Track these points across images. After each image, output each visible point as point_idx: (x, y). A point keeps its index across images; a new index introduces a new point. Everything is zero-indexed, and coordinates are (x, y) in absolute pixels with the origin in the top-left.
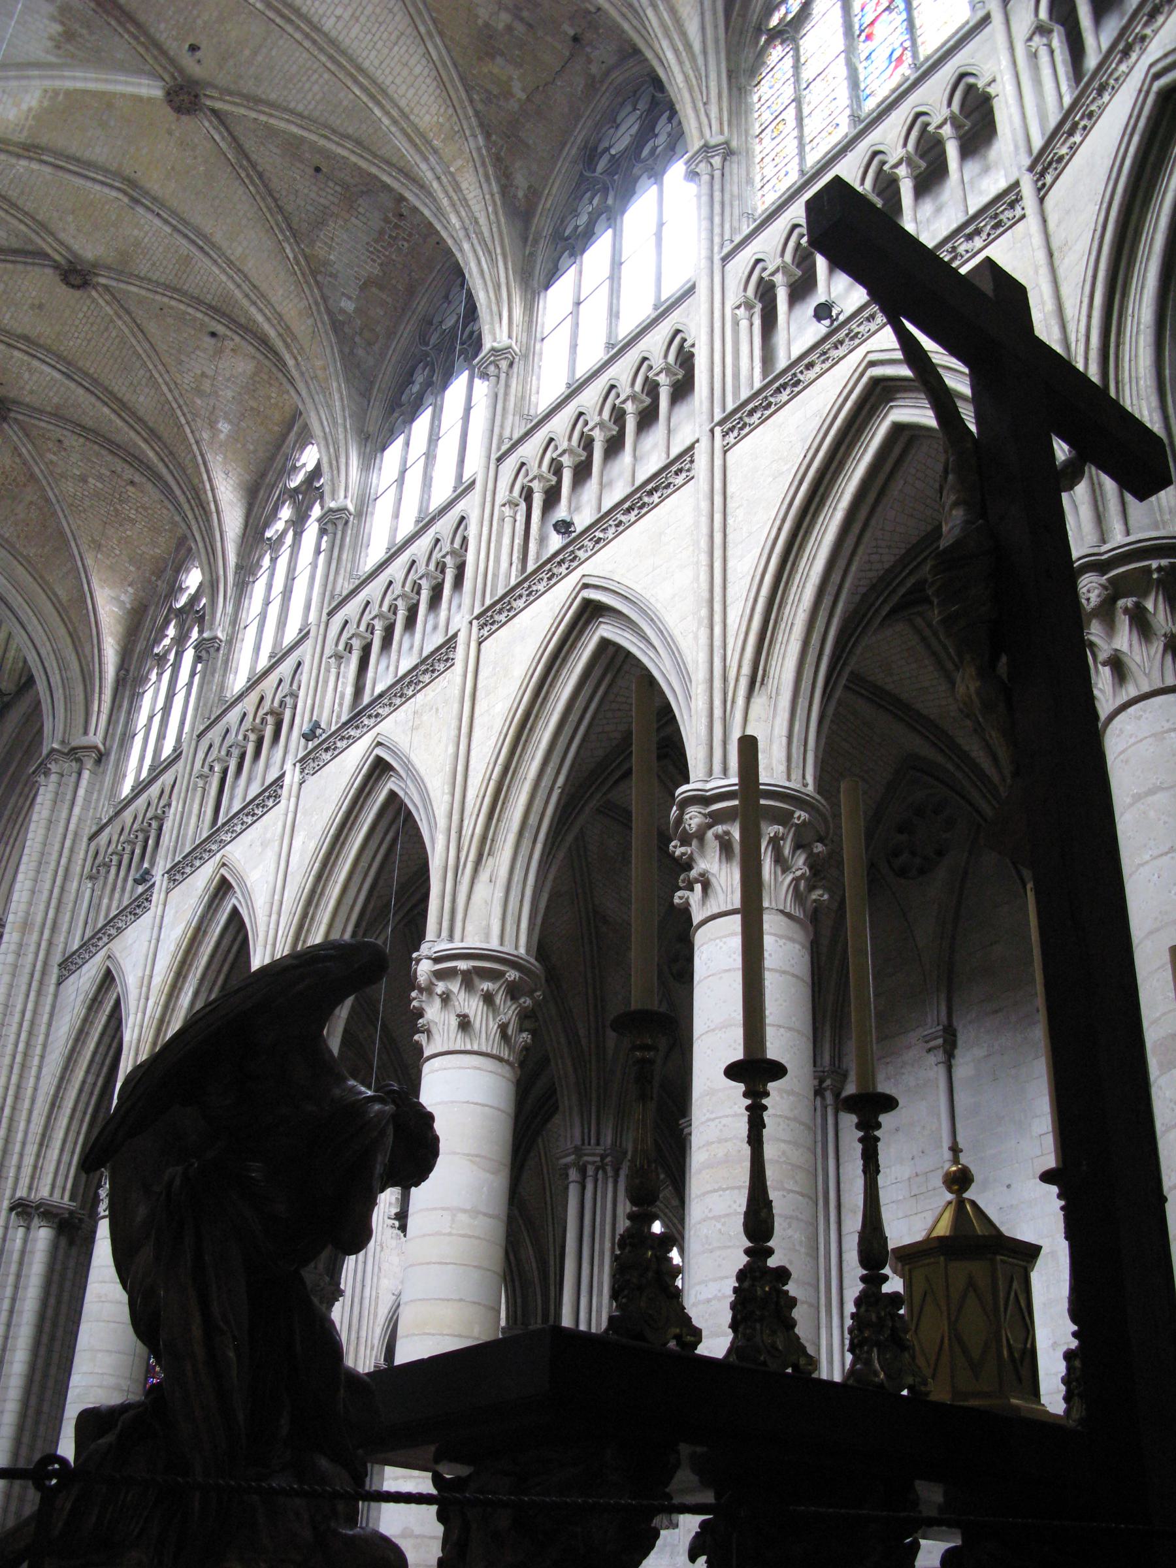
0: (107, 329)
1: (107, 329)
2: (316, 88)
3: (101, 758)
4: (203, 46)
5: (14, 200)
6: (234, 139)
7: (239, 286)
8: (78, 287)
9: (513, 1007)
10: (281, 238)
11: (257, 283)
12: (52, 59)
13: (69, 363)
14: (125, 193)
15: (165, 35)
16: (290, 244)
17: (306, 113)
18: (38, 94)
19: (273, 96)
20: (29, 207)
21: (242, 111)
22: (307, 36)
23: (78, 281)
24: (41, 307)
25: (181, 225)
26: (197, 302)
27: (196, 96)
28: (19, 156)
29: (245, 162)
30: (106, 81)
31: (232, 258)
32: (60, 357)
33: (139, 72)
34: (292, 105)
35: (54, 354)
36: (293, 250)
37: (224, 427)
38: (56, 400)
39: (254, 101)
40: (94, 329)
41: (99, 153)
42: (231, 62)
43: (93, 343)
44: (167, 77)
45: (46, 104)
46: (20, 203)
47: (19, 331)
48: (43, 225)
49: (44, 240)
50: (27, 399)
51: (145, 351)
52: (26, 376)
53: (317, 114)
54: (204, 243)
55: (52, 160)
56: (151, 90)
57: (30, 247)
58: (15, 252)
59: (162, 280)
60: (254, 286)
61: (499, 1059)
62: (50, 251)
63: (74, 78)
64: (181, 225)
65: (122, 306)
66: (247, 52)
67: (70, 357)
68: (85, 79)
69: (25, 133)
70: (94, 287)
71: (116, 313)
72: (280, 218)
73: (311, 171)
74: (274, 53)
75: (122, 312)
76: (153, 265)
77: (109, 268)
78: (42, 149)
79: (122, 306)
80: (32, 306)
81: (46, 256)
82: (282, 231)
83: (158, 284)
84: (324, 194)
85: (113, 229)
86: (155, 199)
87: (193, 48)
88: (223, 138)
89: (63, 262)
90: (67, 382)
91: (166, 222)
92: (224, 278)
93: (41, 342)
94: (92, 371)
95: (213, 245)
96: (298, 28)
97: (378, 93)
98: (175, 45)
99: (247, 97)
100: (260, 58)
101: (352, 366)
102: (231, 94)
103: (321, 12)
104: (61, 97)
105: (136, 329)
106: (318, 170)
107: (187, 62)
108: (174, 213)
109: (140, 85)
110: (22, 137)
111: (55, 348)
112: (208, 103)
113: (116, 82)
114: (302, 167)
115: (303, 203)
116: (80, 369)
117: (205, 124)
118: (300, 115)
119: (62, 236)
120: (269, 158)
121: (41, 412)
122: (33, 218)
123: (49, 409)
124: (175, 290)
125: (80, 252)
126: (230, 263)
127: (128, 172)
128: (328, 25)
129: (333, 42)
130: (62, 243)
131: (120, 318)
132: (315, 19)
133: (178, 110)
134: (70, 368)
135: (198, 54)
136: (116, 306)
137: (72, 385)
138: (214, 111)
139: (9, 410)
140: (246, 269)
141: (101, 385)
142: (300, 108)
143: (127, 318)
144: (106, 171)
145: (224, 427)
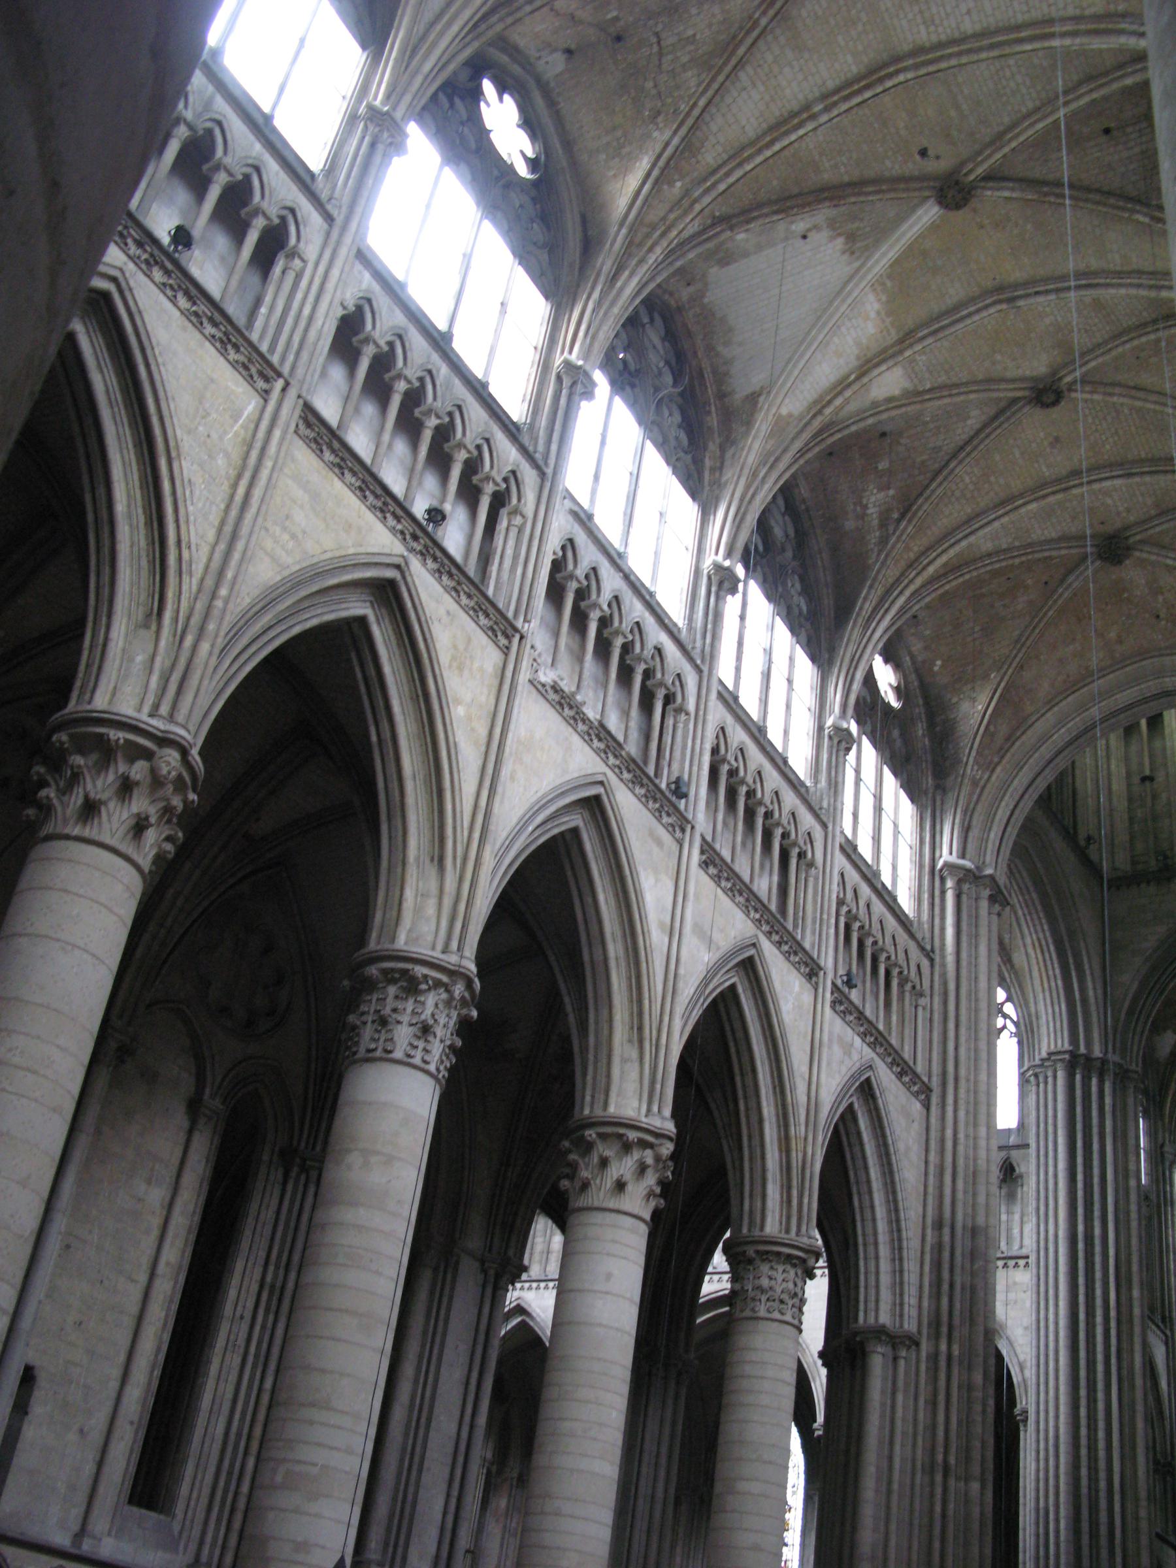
0: (1117, 412)
1: (1117, 412)
2: (1019, 78)
4: (925, 143)
5: (949, 382)
6: (1021, 180)
7: (1139, 286)
8: (1055, 403)
10: (1127, 215)
11: (1151, 269)
12: (857, 264)
13: (1121, 464)
14: (1000, 302)
15: (897, 167)
16: (1138, 212)
17: (1038, 103)
18: (871, 297)
19: (1006, 120)
20: (964, 376)
21: (998, 155)
22: (959, 54)
23: (1052, 397)
24: (1057, 440)
26: (1141, 327)
27: (957, 183)
28: (901, 352)
29: (1045, 189)
30: (898, 240)
31: (1118, 268)
32: (1111, 465)
33: (914, 209)
34: (1024, 110)
36: (1145, 215)
38: (1149, 501)
40: (1109, 419)
41: (955, 292)
42: (955, 133)
43: (1121, 432)
44: (927, 193)
45: (884, 298)
46: (955, 380)
47: (1064, 472)
48: (989, 380)
49: (998, 390)
50: (1132, 518)
51: (1156, 403)
52: (1109, 501)
53: (1044, 95)
55: (926, 332)
56: (929, 213)
57: (1003, 404)
58: (996, 417)
59: (1106, 337)
60: (1152, 273)
62: (1011, 395)
63: (877, 262)
65: (1106, 385)
66: (953, 113)
68: (884, 254)
69: (893, 332)
70: (1070, 390)
71: (1105, 394)
72: (1112, 201)
73: (1103, 139)
74: (966, 91)
75: (1109, 390)
76: (1086, 331)
77: (1065, 365)
78: (911, 332)
79: (1106, 385)
80: (1052, 445)
81: (1015, 401)
82: (1123, 209)
83: (1106, 342)
84: (1132, 143)
85: (1033, 335)
86: (1026, 284)
87: (923, 153)
88: (1013, 189)
89: (1027, 393)
90: (1130, 481)
91: (1047, 292)
92: (1123, 291)
94: (1143, 455)
95: (1095, 274)
96: (950, 56)
98: (910, 165)
99: (992, 143)
100: (964, 107)
102: (979, 153)
103: (954, 26)
104: (889, 284)
105: (1133, 392)
106: (1107, 131)
107: (932, 166)
108: (1046, 280)
109: (920, 218)
110: (894, 336)
112: (972, 177)
113: (904, 234)
114: (1092, 143)
115: (1123, 169)
118: (1037, 110)
119: (1009, 375)
121: (1151, 519)
122: (975, 382)
123: (1153, 512)
124: (1120, 335)
125: (1035, 374)
126: (1119, 274)
127: (989, 284)
128: (968, 27)
129: (983, 34)
130: (1013, 381)
131: (1111, 395)
132: (957, 35)
133: (958, 207)
134: (1124, 467)
135: (930, 152)
137: (1137, 479)
138: (988, 177)
139: (1127, 538)
140: (1135, 267)
141: (1160, 459)
142: (1030, 105)
143: (1117, 390)
144: (972, 300)
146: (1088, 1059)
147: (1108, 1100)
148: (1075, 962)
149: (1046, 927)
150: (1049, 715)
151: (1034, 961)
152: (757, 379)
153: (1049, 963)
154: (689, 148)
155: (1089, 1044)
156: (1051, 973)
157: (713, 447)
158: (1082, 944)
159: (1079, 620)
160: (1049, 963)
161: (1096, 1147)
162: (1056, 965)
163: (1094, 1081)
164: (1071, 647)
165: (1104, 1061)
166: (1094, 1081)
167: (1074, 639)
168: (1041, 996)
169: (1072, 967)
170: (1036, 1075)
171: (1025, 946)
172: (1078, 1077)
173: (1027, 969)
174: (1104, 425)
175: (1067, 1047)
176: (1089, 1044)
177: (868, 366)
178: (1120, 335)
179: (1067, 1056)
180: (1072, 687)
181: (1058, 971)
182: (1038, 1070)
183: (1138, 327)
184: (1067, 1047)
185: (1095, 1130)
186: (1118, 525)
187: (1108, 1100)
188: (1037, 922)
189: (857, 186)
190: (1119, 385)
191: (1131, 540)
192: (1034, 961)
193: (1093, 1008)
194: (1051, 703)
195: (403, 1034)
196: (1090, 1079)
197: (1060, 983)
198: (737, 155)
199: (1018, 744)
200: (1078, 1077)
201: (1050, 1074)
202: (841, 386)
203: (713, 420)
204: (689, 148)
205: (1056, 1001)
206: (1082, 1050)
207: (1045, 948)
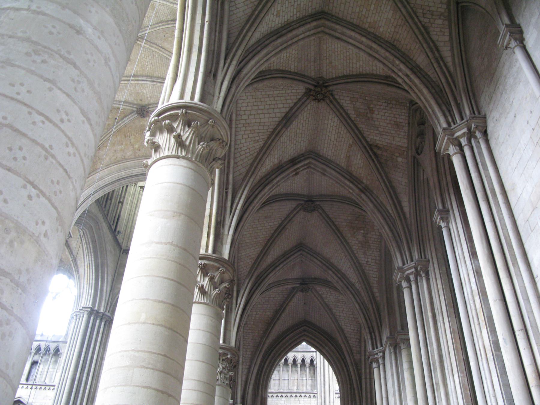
9: (190, 131)
13: (151, 77)
32: (147, 76)
35: (145, 76)
43: (153, 64)
51: (168, 55)
52: (145, 91)
61: (178, 157)
65: (151, 43)
67: (151, 75)
71: (150, 46)
75: (152, 44)
79: (151, 43)
93: (139, 74)
94: (159, 75)
105: (160, 48)
111: (144, 74)
116: (155, 77)
131: (153, 47)
136: (149, 43)
137: (155, 83)
139: (148, 108)
143: (154, 46)
146: (97, 312)
147: (102, 329)
148: (101, 275)
149: (93, 259)
150: (105, 170)
151: (86, 272)
153: (91, 273)
155: (99, 307)
156: (91, 277)
158: (106, 269)
159: (125, 137)
160: (91, 273)
161: (92, 346)
162: (94, 275)
163: (98, 321)
164: (120, 147)
165: (103, 314)
166: (98, 321)
167: (122, 144)
168: (86, 286)
169: (100, 277)
170: (76, 316)
171: (84, 266)
172: (92, 318)
173: (83, 275)
174: (148, 59)
175: (90, 306)
176: (99, 307)
178: (160, 23)
179: (89, 309)
180: (117, 162)
181: (94, 277)
182: (78, 314)
183: (165, 22)
184: (90, 306)
185: (94, 340)
186: (146, 103)
187: (102, 329)
188: (90, 257)
190: (156, 44)
191: (150, 109)
192: (86, 272)
193: (104, 294)
194: (108, 166)
196: (97, 320)
197: (94, 281)
199: (91, 177)
200: (92, 318)
201: (82, 315)
205: (90, 288)
206: (96, 308)
207: (91, 268)
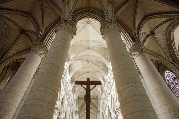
3: (102, 99)
25: (91, 68)
37: (100, 77)
39: (92, 60)
54: (93, 68)
56: (87, 62)
64: (91, 68)
97: (97, 57)
101: (104, 71)
117: (90, 63)
120: (94, 62)
145: (100, 77)
152: (74, 68)
154: (76, 56)
157: (70, 71)
177: (80, 69)
189: (83, 60)
195: (56, 113)
198: (78, 57)
202: (78, 70)
203: (70, 70)
204: (76, 56)
